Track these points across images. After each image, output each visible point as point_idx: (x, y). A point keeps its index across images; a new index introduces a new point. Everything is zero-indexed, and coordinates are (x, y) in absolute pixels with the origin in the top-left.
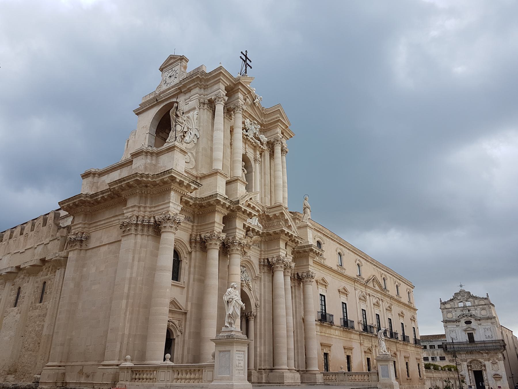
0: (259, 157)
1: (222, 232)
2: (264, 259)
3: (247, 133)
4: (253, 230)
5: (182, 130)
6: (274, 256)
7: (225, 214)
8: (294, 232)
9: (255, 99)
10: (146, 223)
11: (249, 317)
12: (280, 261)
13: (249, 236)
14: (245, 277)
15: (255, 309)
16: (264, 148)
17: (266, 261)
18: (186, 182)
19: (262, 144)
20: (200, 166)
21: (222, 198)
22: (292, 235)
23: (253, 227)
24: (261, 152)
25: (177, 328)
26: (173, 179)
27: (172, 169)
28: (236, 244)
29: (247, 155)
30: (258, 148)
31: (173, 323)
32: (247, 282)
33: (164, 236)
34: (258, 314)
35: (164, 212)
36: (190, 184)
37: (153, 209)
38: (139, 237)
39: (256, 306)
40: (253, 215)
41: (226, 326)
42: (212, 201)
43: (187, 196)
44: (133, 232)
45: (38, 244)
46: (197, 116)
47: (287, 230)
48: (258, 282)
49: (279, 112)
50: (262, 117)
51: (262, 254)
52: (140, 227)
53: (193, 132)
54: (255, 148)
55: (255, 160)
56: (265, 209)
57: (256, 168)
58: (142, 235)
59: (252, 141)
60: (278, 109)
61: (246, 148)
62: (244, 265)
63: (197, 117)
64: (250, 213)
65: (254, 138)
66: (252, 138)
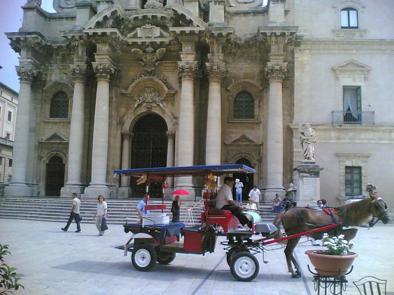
8: (198, 26)
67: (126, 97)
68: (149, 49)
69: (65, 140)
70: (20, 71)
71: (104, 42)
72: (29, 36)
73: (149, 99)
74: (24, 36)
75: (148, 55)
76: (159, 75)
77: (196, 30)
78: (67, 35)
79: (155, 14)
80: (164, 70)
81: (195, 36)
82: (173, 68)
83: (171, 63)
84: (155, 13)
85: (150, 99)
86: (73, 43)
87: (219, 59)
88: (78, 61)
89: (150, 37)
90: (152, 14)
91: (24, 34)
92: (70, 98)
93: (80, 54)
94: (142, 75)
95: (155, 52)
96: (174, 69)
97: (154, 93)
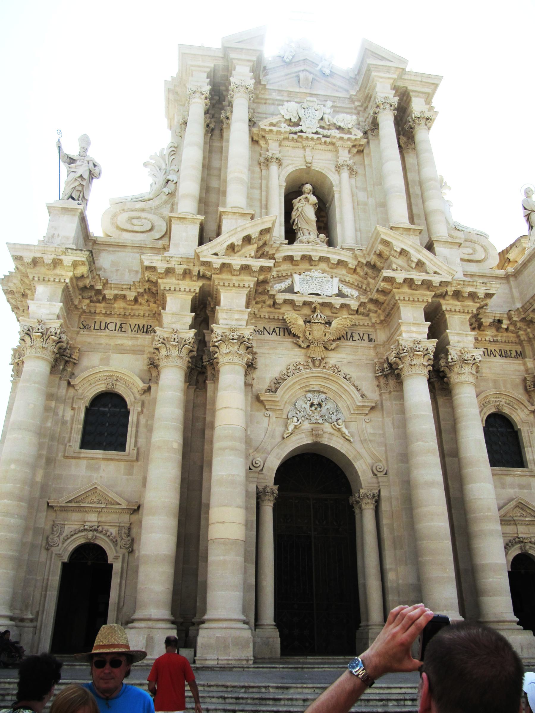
2: (382, 364)
3: (298, 129)
8: (435, 273)
12: (402, 355)
13: (314, 323)
16: (353, 137)
21: (158, 260)
23: (320, 301)
24: (355, 150)
29: (312, 168)
30: (338, 143)
43: (115, 286)
48: (376, 416)
55: (338, 168)
59: (316, 136)
62: (316, 388)
66: (316, 133)
67: (267, 409)
68: (319, 316)
70: (29, 330)
73: (316, 417)
75: (315, 327)
76: (336, 370)
77: (436, 280)
85: (318, 417)
94: (301, 367)
97: (326, 404)
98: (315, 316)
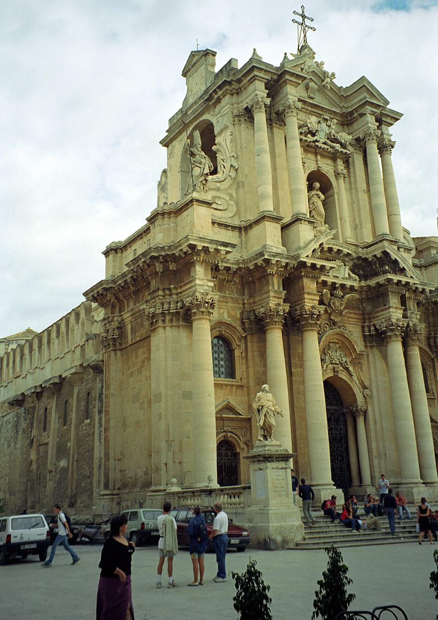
0: (343, 168)
1: (284, 303)
4: (343, 286)
5: (202, 172)
6: (383, 320)
7: (285, 275)
8: (411, 277)
9: (325, 78)
10: (173, 311)
11: (355, 413)
14: (339, 357)
15: (363, 401)
16: (348, 152)
17: (372, 328)
18: (212, 248)
19: (343, 146)
20: (243, 210)
22: (408, 283)
23: (340, 282)
25: (240, 439)
26: (193, 247)
27: (188, 236)
28: (306, 316)
29: (321, 171)
31: (233, 433)
32: (343, 365)
33: (196, 324)
34: (370, 409)
35: (191, 294)
36: (219, 248)
37: (179, 291)
38: (168, 329)
39: (364, 397)
40: (328, 268)
41: (260, 440)
42: (260, 262)
44: (160, 324)
45: (74, 347)
46: (231, 137)
47: (395, 278)
49: (365, 90)
50: (342, 101)
51: (365, 319)
52: (168, 318)
53: (227, 163)
54: (334, 157)
56: (360, 250)
57: (340, 188)
58: (171, 327)
59: (326, 147)
60: (363, 85)
61: (317, 161)
63: (232, 139)
64: (323, 267)
65: (328, 141)
66: (325, 143)
69: (241, 415)
71: (314, 277)
72: (222, 248)
74: (215, 246)
78: (272, 258)
79: (341, 249)
80: (347, 322)
81: (404, 288)
82: (355, 320)
83: (355, 314)
84: (342, 246)
86: (270, 270)
87: (417, 319)
88: (275, 297)
89: (337, 277)
90: (338, 248)
91: (216, 244)
92: (236, 348)
93: (276, 287)
95: (343, 297)
96: (356, 322)
98: (337, 293)
